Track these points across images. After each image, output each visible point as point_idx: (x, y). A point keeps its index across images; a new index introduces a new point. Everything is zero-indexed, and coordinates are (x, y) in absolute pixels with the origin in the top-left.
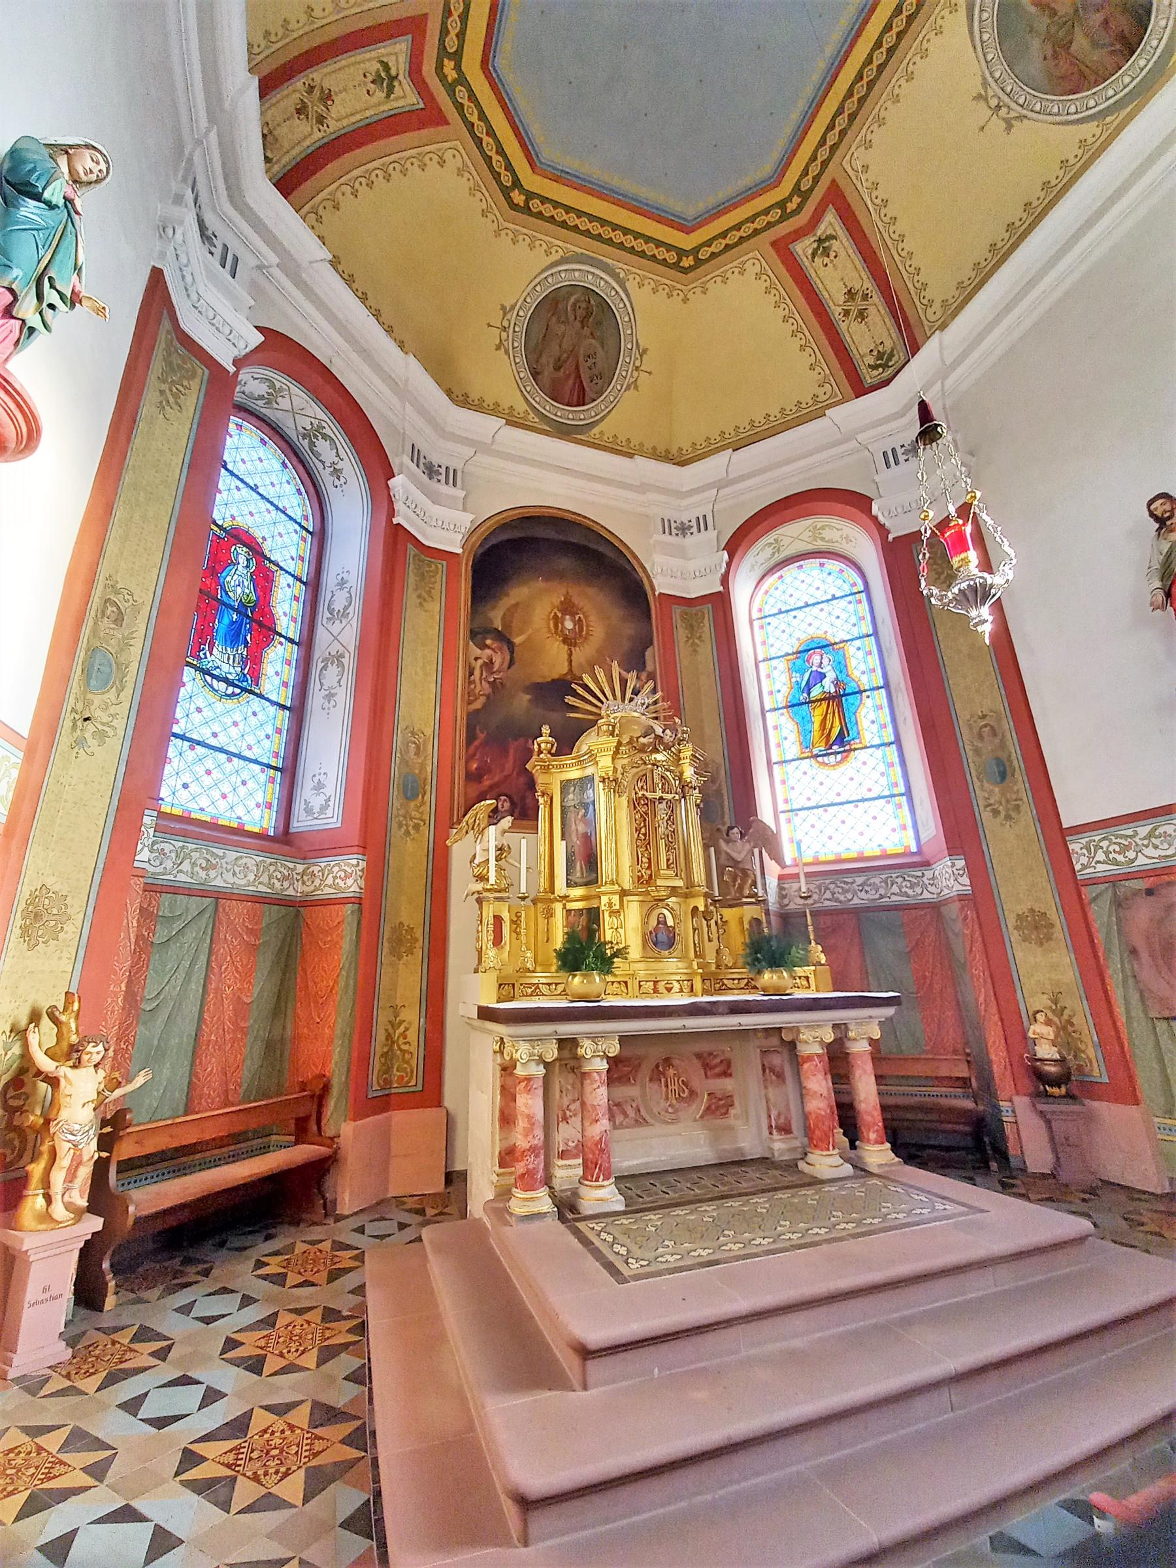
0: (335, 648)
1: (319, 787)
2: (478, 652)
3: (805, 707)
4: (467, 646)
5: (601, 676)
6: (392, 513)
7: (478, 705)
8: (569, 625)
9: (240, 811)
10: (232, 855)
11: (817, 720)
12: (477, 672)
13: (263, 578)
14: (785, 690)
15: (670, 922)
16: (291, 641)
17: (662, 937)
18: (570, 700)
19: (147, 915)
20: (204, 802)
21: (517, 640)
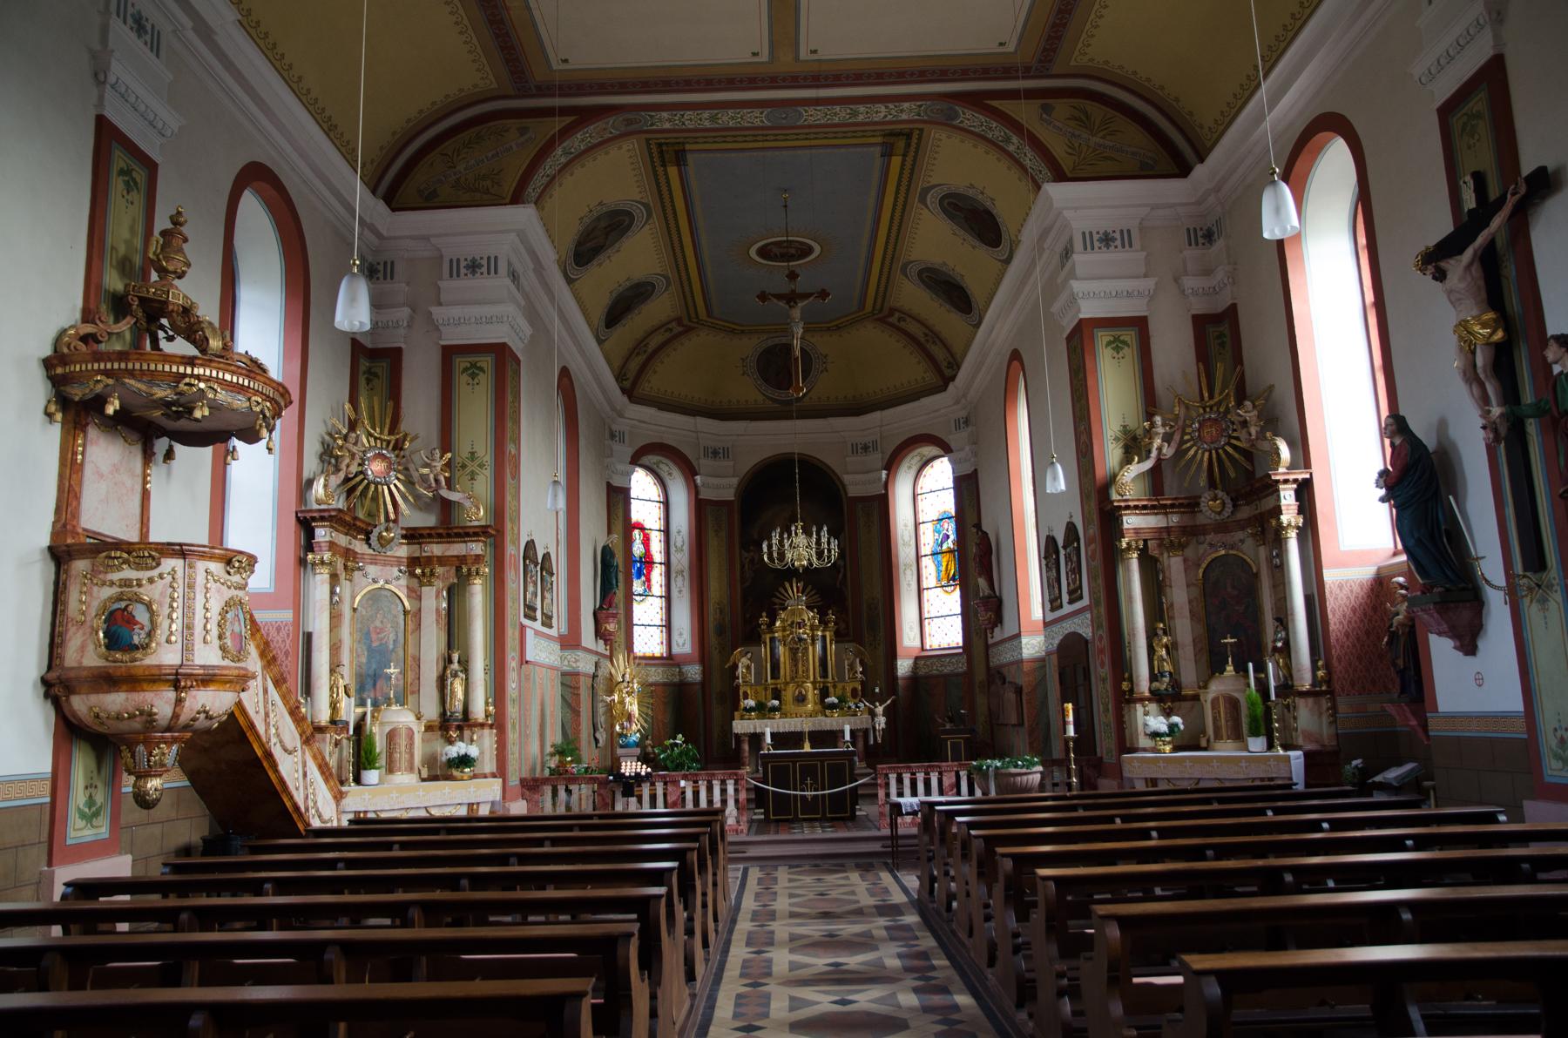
0: (679, 567)
1: (681, 634)
2: (746, 554)
3: (939, 556)
4: (741, 555)
5: (783, 591)
6: (697, 493)
7: (747, 584)
9: (652, 649)
10: (653, 669)
11: (944, 564)
12: (746, 566)
13: (646, 542)
14: (932, 543)
15: (804, 692)
16: (661, 564)
18: (787, 585)
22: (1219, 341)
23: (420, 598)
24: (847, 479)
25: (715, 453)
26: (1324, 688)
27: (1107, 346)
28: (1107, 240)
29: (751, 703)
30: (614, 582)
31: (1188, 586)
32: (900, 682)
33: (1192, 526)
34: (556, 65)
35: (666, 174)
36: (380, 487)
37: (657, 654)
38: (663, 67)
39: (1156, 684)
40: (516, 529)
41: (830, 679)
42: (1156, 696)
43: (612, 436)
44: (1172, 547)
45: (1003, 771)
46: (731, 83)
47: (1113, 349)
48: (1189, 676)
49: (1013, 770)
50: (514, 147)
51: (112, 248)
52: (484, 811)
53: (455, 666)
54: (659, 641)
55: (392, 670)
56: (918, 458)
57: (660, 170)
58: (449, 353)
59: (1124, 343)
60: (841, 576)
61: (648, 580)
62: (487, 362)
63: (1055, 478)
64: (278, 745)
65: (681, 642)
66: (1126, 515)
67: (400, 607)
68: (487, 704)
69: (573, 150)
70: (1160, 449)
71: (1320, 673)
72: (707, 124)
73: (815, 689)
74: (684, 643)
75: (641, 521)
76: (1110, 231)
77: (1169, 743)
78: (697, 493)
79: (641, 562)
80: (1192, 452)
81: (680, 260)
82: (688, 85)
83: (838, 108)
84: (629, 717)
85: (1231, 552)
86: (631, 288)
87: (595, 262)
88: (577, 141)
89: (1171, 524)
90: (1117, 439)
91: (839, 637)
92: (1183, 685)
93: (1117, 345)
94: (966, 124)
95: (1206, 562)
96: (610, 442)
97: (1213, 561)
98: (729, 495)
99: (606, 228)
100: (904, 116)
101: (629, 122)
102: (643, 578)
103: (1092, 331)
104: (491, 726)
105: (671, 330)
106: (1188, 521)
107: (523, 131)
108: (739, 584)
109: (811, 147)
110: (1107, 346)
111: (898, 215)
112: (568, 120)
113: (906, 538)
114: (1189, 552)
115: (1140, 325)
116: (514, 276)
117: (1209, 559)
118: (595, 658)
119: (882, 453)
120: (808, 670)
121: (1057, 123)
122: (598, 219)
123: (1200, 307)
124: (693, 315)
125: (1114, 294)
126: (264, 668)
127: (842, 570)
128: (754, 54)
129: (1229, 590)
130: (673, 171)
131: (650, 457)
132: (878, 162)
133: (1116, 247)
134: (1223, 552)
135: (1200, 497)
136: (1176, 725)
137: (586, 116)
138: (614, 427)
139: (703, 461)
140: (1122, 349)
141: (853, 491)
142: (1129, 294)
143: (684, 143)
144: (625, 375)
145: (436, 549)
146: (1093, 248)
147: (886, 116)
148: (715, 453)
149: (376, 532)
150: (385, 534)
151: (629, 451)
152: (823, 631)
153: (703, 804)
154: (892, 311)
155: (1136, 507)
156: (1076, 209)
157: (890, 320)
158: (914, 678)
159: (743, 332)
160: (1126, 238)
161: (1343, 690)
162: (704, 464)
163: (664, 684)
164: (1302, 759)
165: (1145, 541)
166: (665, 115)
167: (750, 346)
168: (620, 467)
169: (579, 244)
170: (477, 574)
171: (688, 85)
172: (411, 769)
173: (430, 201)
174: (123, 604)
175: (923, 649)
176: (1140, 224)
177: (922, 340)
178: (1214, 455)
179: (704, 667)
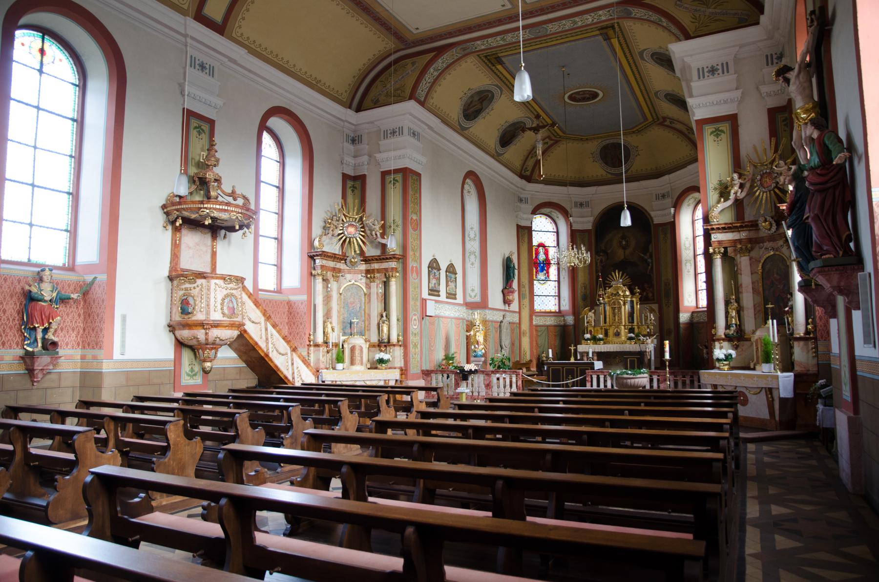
1: (564, 300)
2: (598, 258)
5: (611, 277)
6: (571, 226)
8: (624, 243)
9: (550, 307)
12: (598, 264)
13: (546, 253)
17: (617, 334)
19: (536, 330)
20: (543, 307)
21: (609, 252)
22: (783, 123)
23: (370, 288)
24: (653, 214)
25: (581, 205)
26: (811, 336)
27: (710, 135)
28: (713, 71)
29: (588, 336)
30: (512, 275)
31: (752, 274)
32: (681, 326)
33: (756, 238)
34: (415, 32)
35: (497, 69)
36: (352, 239)
37: (553, 310)
38: (463, 21)
39: (728, 331)
40: (418, 255)
41: (635, 323)
42: (728, 338)
43: (521, 200)
44: (741, 251)
45: (620, 376)
46: (490, 24)
47: (715, 136)
48: (749, 324)
49: (625, 376)
50: (410, 73)
51: (192, 159)
52: (392, 383)
53: (385, 318)
54: (554, 304)
55: (355, 320)
56: (693, 200)
57: (493, 68)
58: (385, 174)
59: (722, 131)
60: (650, 267)
61: (548, 272)
62: (399, 177)
63: (625, 218)
64: (275, 351)
65: (564, 304)
66: (713, 233)
67: (362, 292)
68: (398, 335)
69: (439, 68)
70: (736, 193)
71: (810, 327)
72: (502, 43)
73: (625, 329)
74: (566, 306)
75: (543, 242)
76: (715, 65)
77: (726, 365)
78: (571, 226)
79: (543, 263)
80: (757, 193)
81: (532, 109)
82: (480, 27)
83: (564, 22)
84: (478, 343)
85: (777, 253)
86: (510, 126)
87: (480, 117)
88: (440, 63)
89: (742, 237)
90: (715, 189)
91: (643, 300)
92: (746, 332)
93: (717, 133)
94: (638, 15)
95: (764, 259)
96: (519, 204)
97: (767, 258)
98: (589, 226)
99: (479, 100)
100: (603, 18)
101: (464, 49)
102: (545, 272)
103: (702, 127)
104: (400, 346)
105: (547, 143)
106: (753, 235)
107: (413, 64)
108: (594, 273)
109: (547, 47)
110: (710, 135)
111: (634, 68)
112: (433, 54)
113: (687, 245)
114: (753, 254)
115: (732, 120)
116: (414, 134)
117: (765, 257)
118: (502, 313)
119: (672, 198)
120: (621, 319)
121: (686, 5)
122: (472, 96)
123: (772, 103)
124: (556, 134)
125: (715, 103)
126: (265, 320)
127: (650, 264)
128: (503, 6)
129: (775, 276)
130: (499, 67)
131: (545, 209)
132: (604, 43)
133: (719, 74)
134: (772, 253)
135: (758, 221)
136: (731, 355)
137: (440, 51)
138: (522, 196)
139: (574, 210)
140: (720, 135)
141: (657, 221)
142: (726, 102)
143: (497, 54)
144: (526, 168)
145: (376, 266)
146: (704, 77)
147: (593, 20)
148: (581, 205)
149: (348, 259)
150: (353, 260)
151: (531, 208)
152: (631, 298)
153: (602, 386)
154: (665, 119)
155: (718, 229)
156: (691, 56)
157: (666, 123)
158: (691, 324)
159: (587, 139)
160: (725, 68)
161: (822, 337)
162: (575, 211)
163: (555, 326)
164: (792, 378)
165: (726, 248)
166: (479, 42)
167: (594, 146)
168: (525, 216)
169: (464, 111)
170: (392, 276)
171: (480, 27)
172: (362, 364)
173: (377, 104)
174: (185, 297)
175: (697, 307)
176: (735, 57)
177: (686, 132)
178: (768, 195)
179: (575, 317)
